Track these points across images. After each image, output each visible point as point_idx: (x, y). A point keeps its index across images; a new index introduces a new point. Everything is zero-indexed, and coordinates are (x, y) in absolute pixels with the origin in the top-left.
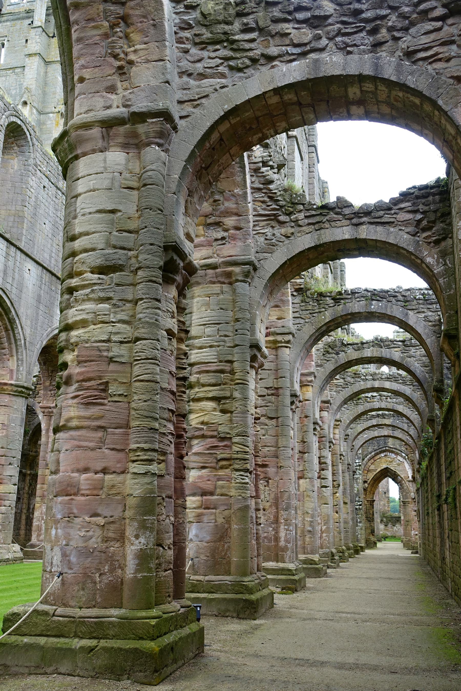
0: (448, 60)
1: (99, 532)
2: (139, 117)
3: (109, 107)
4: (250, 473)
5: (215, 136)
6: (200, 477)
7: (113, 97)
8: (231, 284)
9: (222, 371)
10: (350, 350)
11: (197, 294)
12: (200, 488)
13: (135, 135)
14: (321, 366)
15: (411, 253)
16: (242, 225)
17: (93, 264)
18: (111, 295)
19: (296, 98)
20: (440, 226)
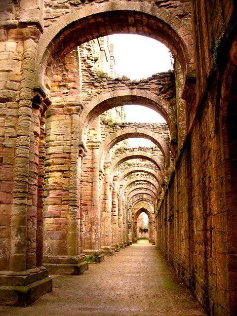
0: (176, 7)
2: (24, 25)
4: (78, 207)
5: (62, 37)
7: (11, 14)
8: (70, 115)
9: (64, 158)
10: (128, 152)
13: (21, 34)
14: (114, 159)
15: (157, 103)
16: (76, 87)
18: (6, 113)
19: (103, 21)
20: (170, 92)
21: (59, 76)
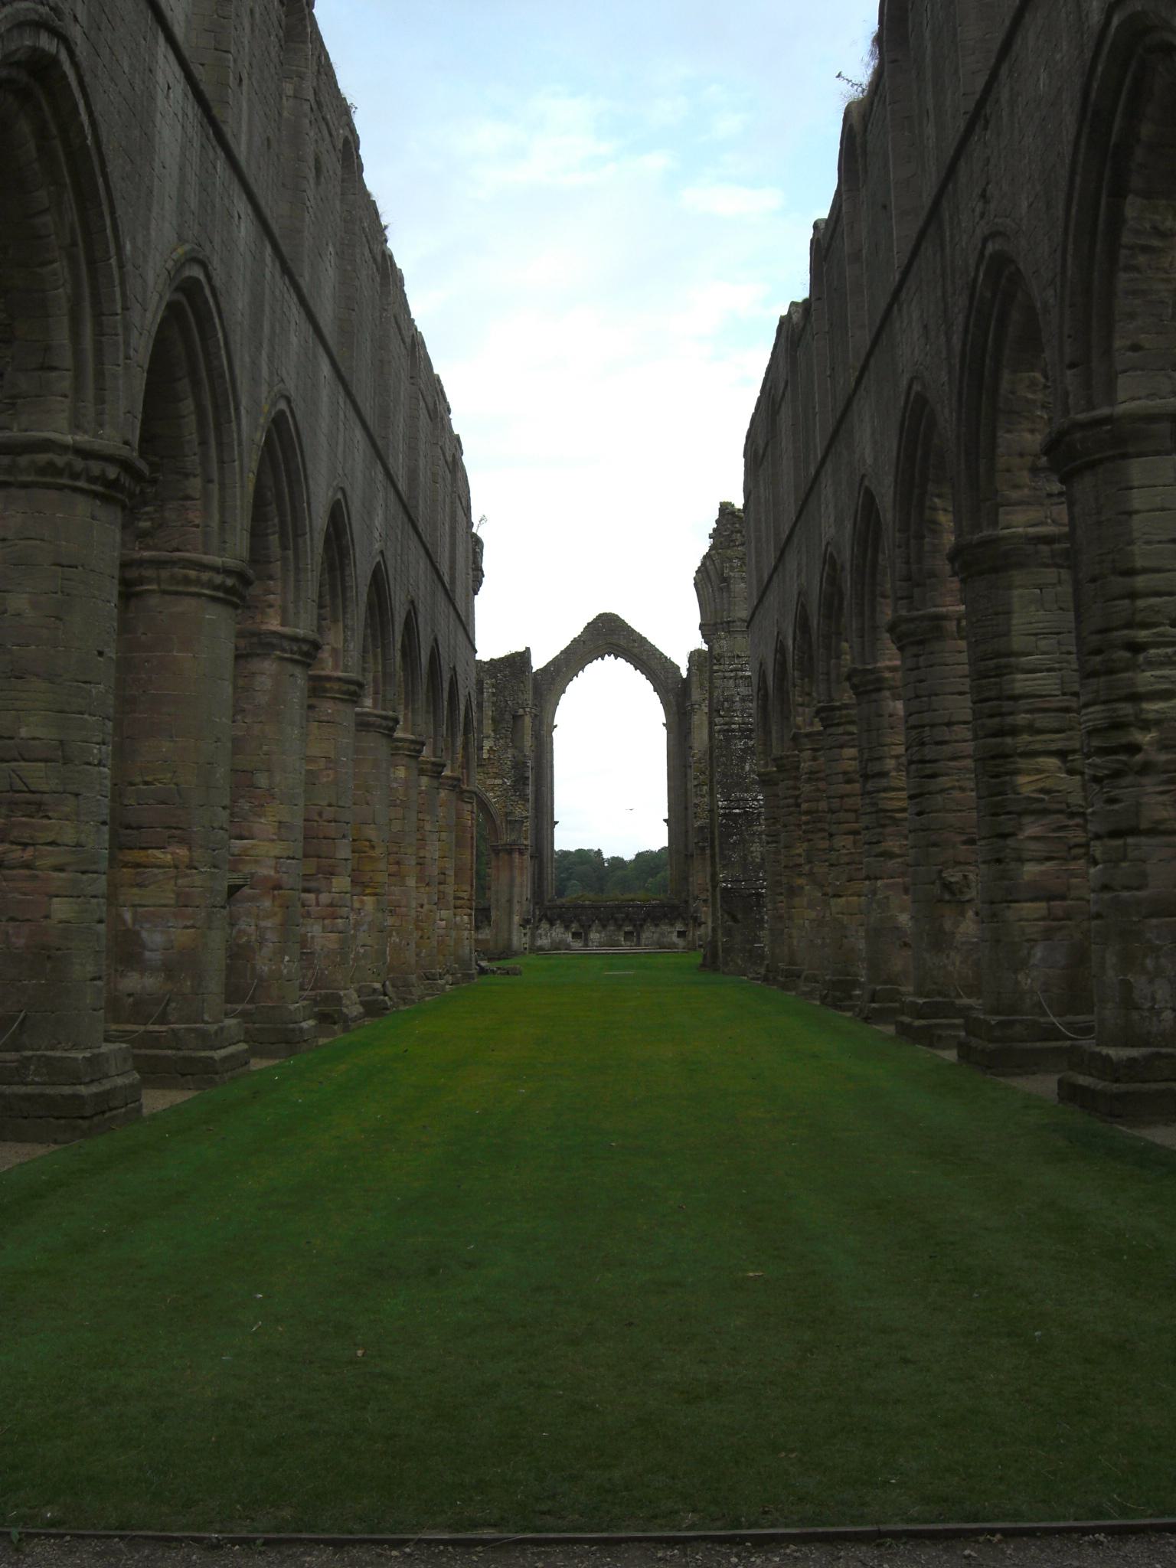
9: (1067, 710)
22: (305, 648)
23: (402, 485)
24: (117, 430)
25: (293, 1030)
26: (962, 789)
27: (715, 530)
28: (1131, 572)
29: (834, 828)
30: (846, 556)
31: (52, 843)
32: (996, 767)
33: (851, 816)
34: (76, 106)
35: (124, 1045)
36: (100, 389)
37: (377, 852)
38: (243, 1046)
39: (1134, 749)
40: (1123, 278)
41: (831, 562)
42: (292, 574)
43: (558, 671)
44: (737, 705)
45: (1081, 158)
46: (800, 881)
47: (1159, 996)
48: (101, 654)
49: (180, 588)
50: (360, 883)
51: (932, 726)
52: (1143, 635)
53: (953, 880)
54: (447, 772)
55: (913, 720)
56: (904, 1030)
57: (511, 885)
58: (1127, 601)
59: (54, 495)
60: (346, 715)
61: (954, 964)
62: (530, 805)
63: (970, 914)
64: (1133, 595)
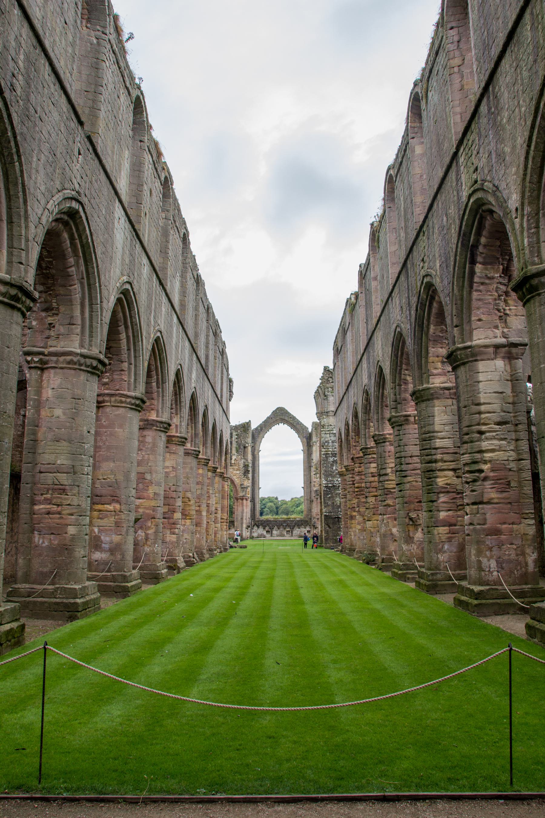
1: (514, 552)
3: (496, 337)
6: (447, 516)
7: (497, 331)
9: (456, 453)
11: (437, 405)
12: (449, 522)
13: (510, 353)
17: (496, 421)
18: (506, 437)
21: (444, 350)
22: (165, 426)
23: (203, 362)
24: (97, 349)
25: (159, 573)
26: (416, 481)
27: (322, 377)
28: (479, 404)
29: (367, 494)
30: (372, 391)
31: (69, 505)
32: (429, 474)
33: (374, 490)
34: (85, 228)
35: (94, 582)
36: (91, 332)
37: (192, 502)
38: (140, 581)
39: (481, 471)
40: (475, 295)
41: (366, 392)
42: (161, 398)
43: (261, 430)
44: (330, 444)
45: (459, 250)
46: (354, 514)
47: (492, 566)
48: (89, 432)
49: (119, 405)
50: (185, 515)
51: (405, 457)
52: (484, 428)
53: (413, 516)
54: (218, 470)
55: (397, 455)
56: (395, 574)
57: (242, 513)
58: (478, 415)
59: (73, 372)
60: (181, 450)
61: (414, 549)
62: (250, 481)
63: (420, 530)
64: (480, 413)
